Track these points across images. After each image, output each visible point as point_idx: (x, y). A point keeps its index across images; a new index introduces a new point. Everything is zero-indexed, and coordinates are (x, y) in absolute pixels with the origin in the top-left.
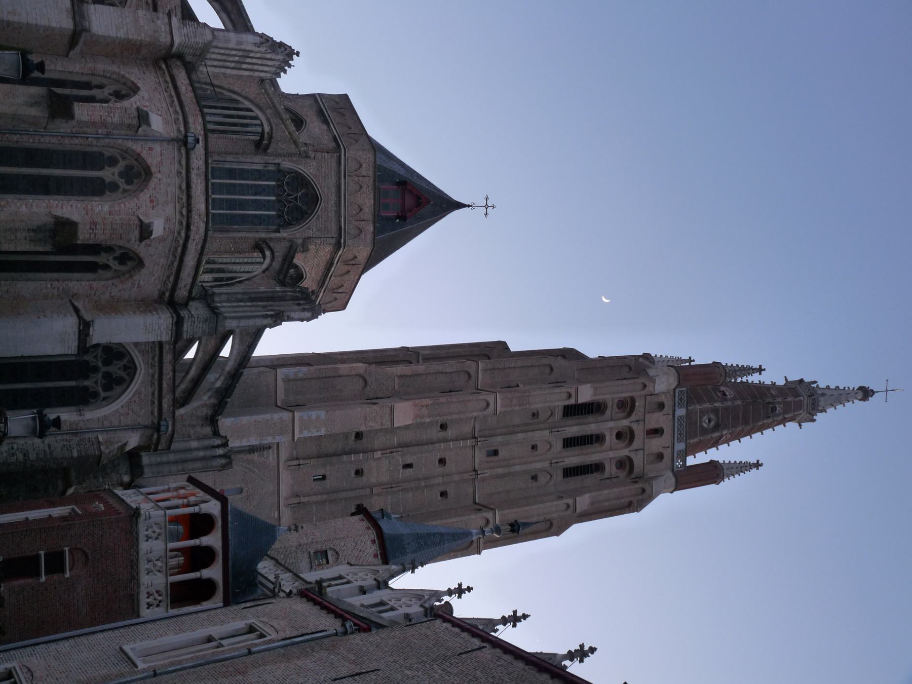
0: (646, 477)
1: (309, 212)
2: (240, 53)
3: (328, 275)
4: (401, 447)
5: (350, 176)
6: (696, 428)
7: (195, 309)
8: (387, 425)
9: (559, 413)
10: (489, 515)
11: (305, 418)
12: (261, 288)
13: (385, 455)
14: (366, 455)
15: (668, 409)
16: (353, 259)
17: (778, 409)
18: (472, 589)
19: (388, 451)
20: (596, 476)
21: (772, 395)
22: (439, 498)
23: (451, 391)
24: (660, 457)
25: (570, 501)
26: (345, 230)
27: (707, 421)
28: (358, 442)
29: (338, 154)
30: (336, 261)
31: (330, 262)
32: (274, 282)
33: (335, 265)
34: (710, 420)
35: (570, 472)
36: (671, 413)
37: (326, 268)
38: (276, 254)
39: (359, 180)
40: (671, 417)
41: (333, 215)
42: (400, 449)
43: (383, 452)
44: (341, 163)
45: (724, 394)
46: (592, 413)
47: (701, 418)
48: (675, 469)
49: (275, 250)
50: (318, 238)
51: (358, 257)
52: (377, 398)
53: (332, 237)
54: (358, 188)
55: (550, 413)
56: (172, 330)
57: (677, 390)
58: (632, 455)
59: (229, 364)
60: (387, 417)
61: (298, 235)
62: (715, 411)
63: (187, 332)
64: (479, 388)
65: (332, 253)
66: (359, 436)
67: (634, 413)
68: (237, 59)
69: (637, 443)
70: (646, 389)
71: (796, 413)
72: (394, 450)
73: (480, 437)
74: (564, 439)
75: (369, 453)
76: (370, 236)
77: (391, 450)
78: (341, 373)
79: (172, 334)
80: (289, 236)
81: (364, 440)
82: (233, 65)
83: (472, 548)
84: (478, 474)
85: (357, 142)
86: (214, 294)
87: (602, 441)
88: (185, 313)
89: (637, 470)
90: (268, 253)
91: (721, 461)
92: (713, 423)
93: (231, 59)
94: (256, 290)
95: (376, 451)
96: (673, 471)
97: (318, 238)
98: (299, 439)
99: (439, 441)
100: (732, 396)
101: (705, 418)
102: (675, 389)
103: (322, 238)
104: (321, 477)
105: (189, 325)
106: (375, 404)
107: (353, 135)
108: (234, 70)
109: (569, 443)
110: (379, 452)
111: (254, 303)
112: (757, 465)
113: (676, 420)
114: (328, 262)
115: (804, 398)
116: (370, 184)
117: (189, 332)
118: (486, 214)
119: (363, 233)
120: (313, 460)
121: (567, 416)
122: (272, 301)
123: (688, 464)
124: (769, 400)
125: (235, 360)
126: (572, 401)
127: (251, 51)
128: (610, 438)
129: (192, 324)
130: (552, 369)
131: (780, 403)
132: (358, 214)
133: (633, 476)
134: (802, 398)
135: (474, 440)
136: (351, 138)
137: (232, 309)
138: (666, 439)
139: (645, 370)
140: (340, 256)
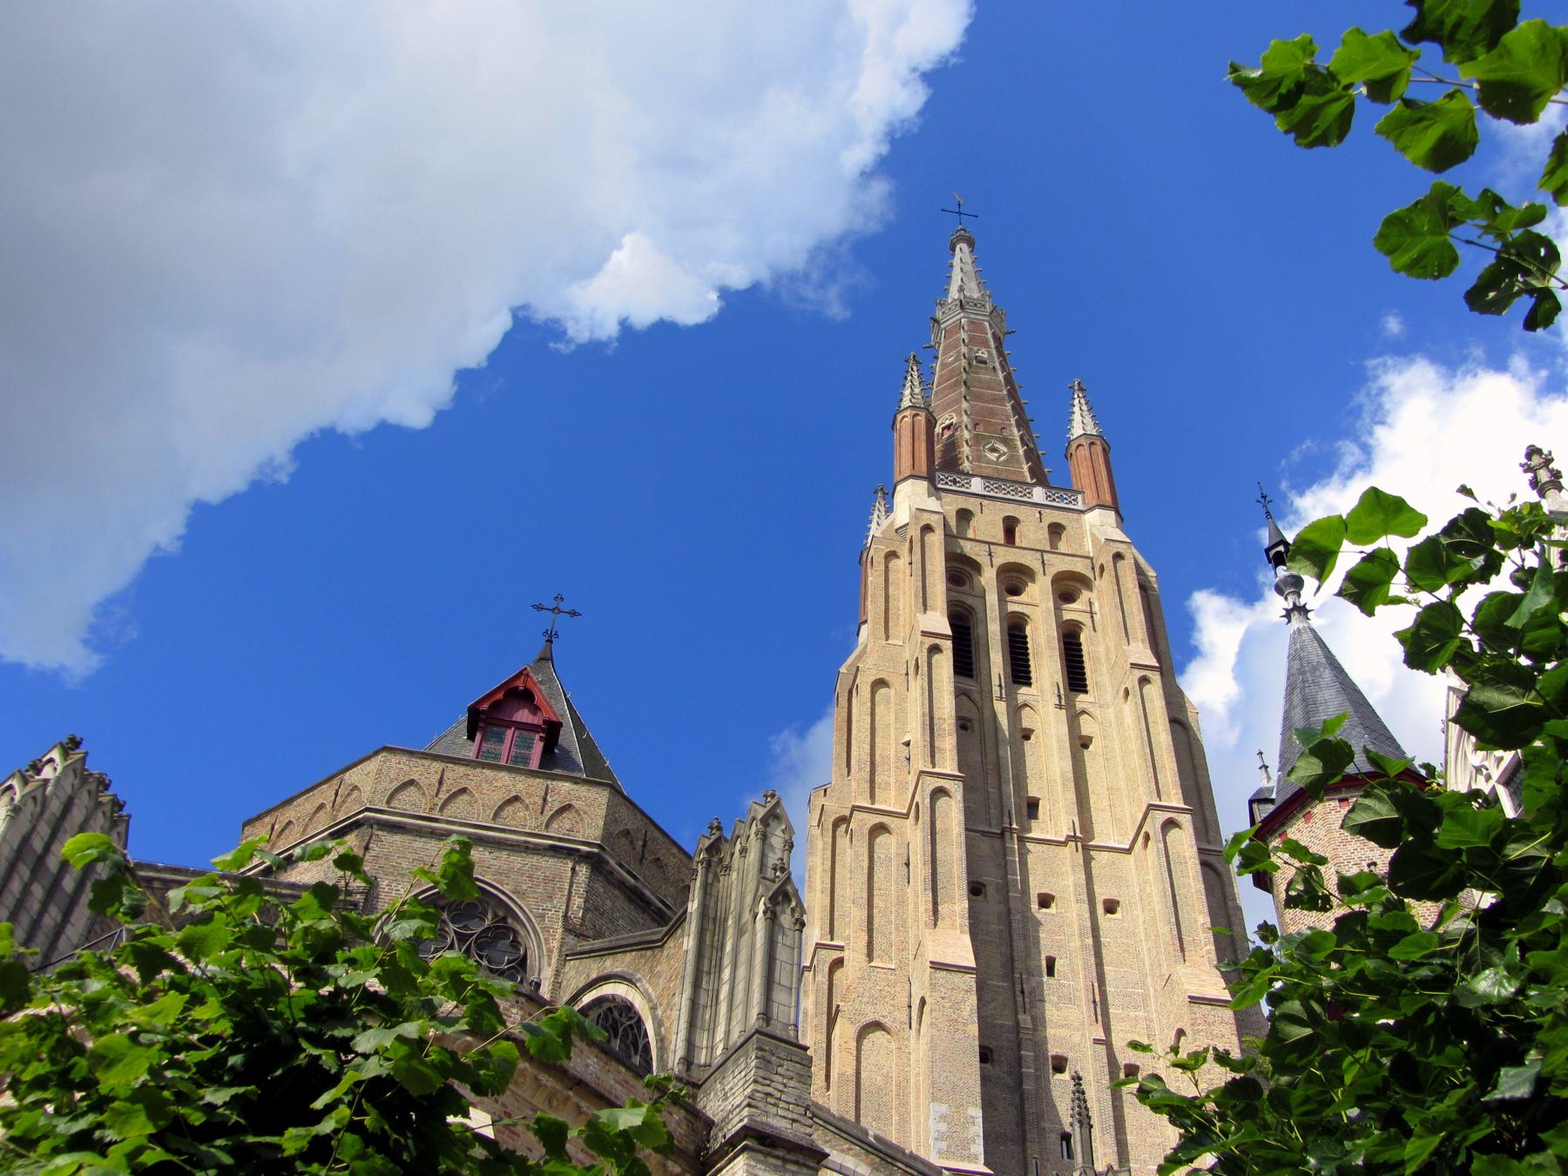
0: (1091, 555)
1: (501, 914)
2: (24, 871)
3: (660, 909)
4: (1013, 973)
5: (431, 809)
6: (1006, 470)
7: (727, 1098)
8: (970, 980)
9: (968, 684)
11: (943, 1145)
12: (685, 948)
13: (1027, 1006)
14: (1024, 1044)
15: (971, 504)
16: (632, 842)
17: (980, 354)
18: (1532, 451)
19: (1019, 999)
21: (957, 359)
22: (1118, 915)
23: (908, 865)
24: (1056, 530)
26: (560, 840)
27: (997, 455)
28: (995, 1056)
29: (375, 826)
30: (632, 881)
31: (628, 892)
32: (671, 944)
33: (639, 885)
34: (993, 450)
35: (1075, 678)
36: (980, 500)
37: (644, 911)
38: (594, 975)
39: (448, 791)
40: (985, 502)
41: (519, 860)
42: (1017, 975)
43: (1020, 1009)
44: (399, 822)
45: (948, 427)
46: (968, 628)
47: (989, 461)
48: (1080, 506)
49: (582, 982)
50: (569, 900)
51: (627, 827)
52: (910, 1007)
53: (573, 869)
54: (465, 797)
55: (964, 697)
56: (785, 1160)
57: (940, 486)
58: (1051, 572)
59: (852, 1167)
60: (957, 978)
61: (556, 944)
62: (977, 440)
63: (794, 1120)
64: (905, 812)
65: (610, 883)
66: (985, 1056)
67: (974, 557)
68: (38, 891)
69: (1030, 560)
70: (933, 524)
72: (1018, 987)
73: (1002, 822)
74: (1014, 682)
75: (1021, 1036)
76: (583, 790)
77: (1018, 993)
78: (851, 1070)
79: (796, 1163)
80: (554, 960)
81: (993, 1044)
82: (54, 913)
83: (1218, 866)
84: (1075, 836)
85: (355, 788)
86: (688, 1060)
87: (1020, 618)
88: (737, 1119)
89: (1080, 567)
90: (587, 998)
92: (1003, 448)
93: (35, 907)
94: (691, 957)
95: (1017, 1023)
96: (1082, 512)
97: (569, 900)
98: (986, 1164)
99: (1006, 900)
100: (954, 415)
101: (993, 456)
103: (570, 893)
104: (1064, 1143)
105: (774, 1110)
106: (923, 1002)
107: (338, 798)
108: (73, 919)
110: (1021, 1017)
111: (727, 960)
113: (992, 494)
114: (630, 900)
115: (964, 317)
116: (461, 770)
117: (795, 1116)
118: (573, 614)
119: (573, 803)
120: (1029, 1151)
121: (971, 670)
122: (726, 920)
124: (964, 363)
125: (842, 1151)
126: (948, 645)
127: (26, 840)
129: (772, 1100)
130: (880, 683)
131: (971, 350)
132: (527, 808)
133: (1091, 576)
135: (1007, 834)
136: (344, 802)
137: (738, 1013)
139: (897, 530)
140: (621, 866)
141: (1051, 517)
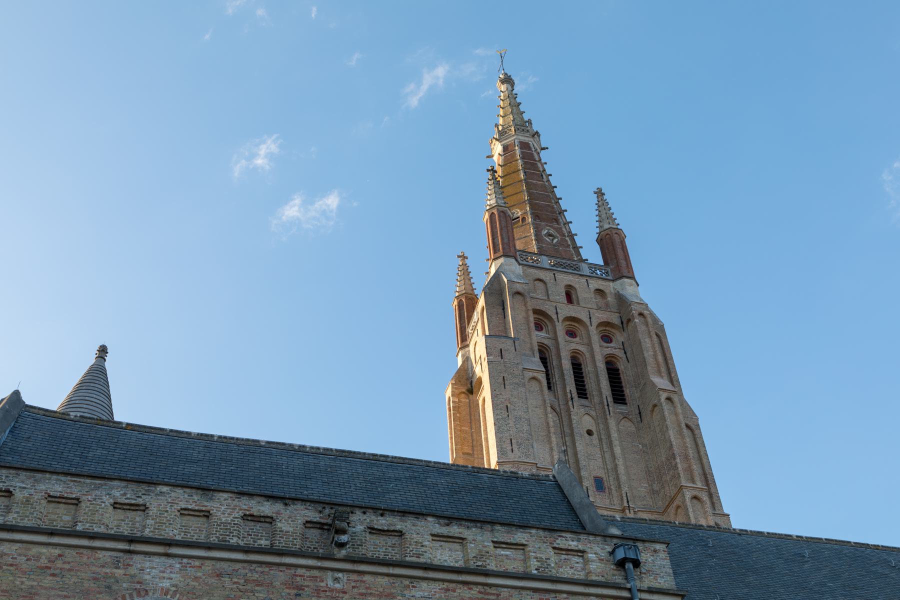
10: (688, 495)
15: (542, 275)
20: (621, 366)
25: (664, 396)
34: (549, 235)
35: (619, 396)
58: (595, 322)
71: (533, 150)
84: (629, 506)
91: (598, 230)
102: (519, 264)
109: (582, 392)
112: (600, 193)
123: (602, 264)
128: (576, 344)
134: (516, 141)
138: (578, 283)
141: (594, 284)
